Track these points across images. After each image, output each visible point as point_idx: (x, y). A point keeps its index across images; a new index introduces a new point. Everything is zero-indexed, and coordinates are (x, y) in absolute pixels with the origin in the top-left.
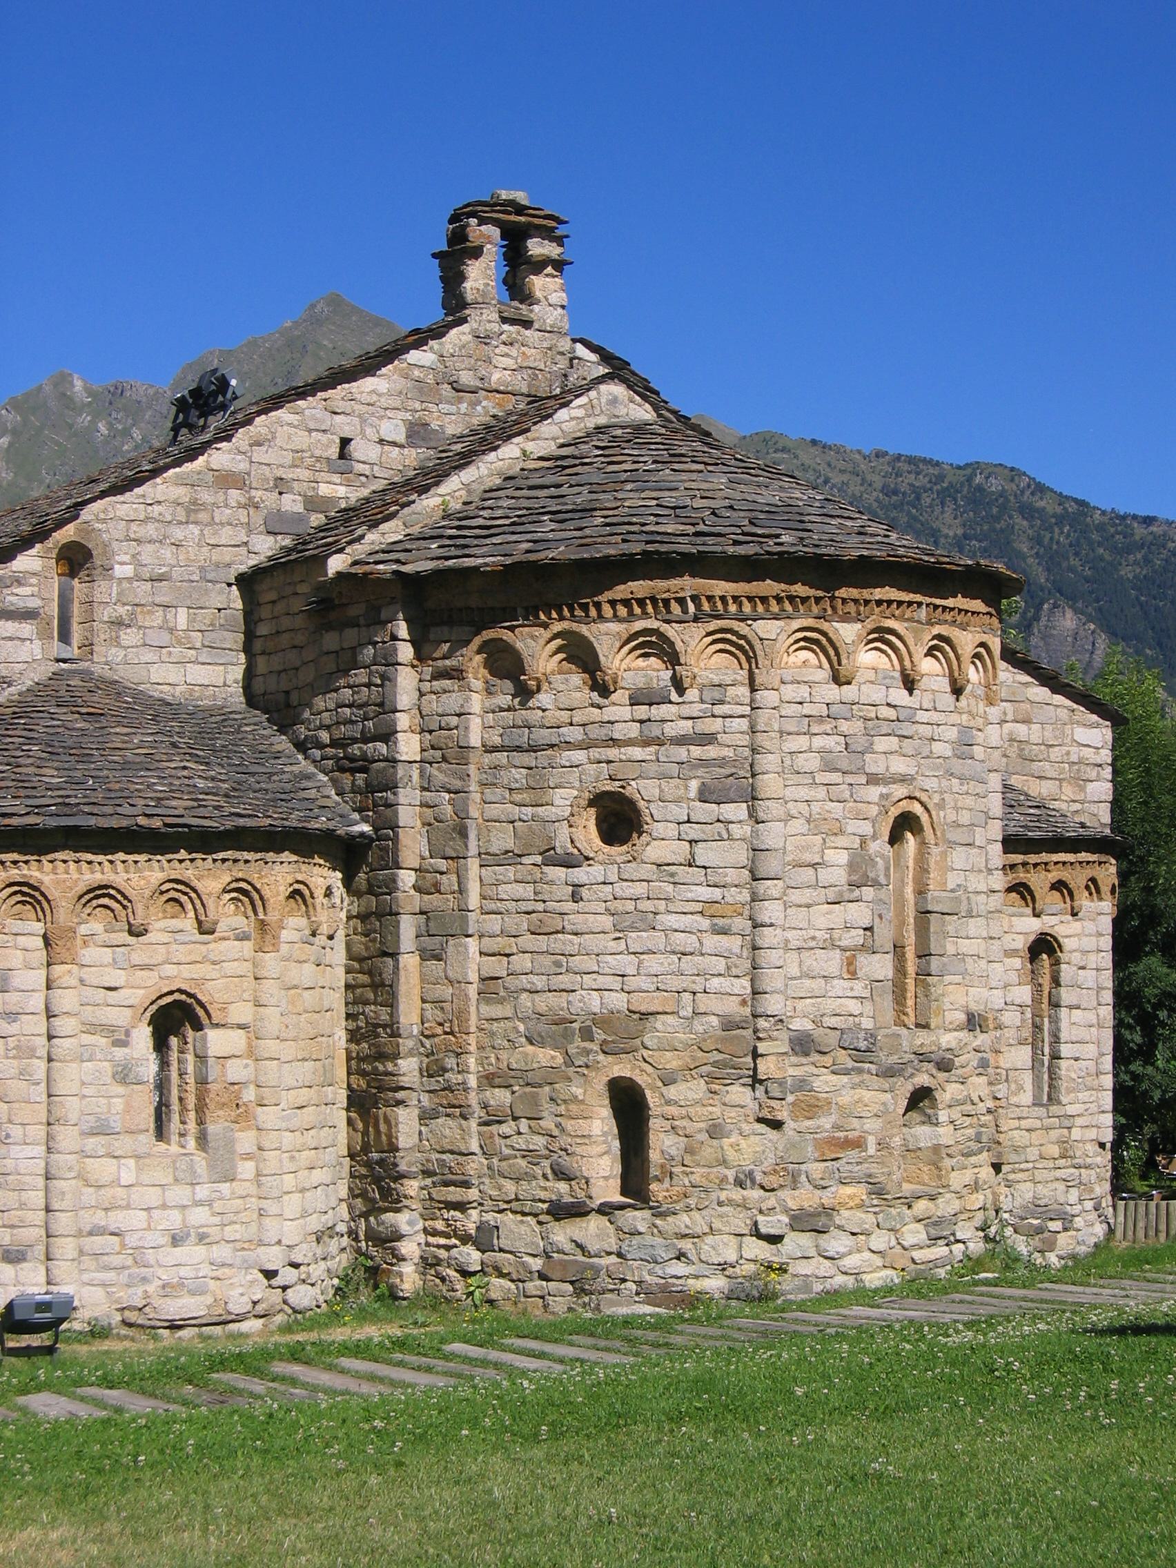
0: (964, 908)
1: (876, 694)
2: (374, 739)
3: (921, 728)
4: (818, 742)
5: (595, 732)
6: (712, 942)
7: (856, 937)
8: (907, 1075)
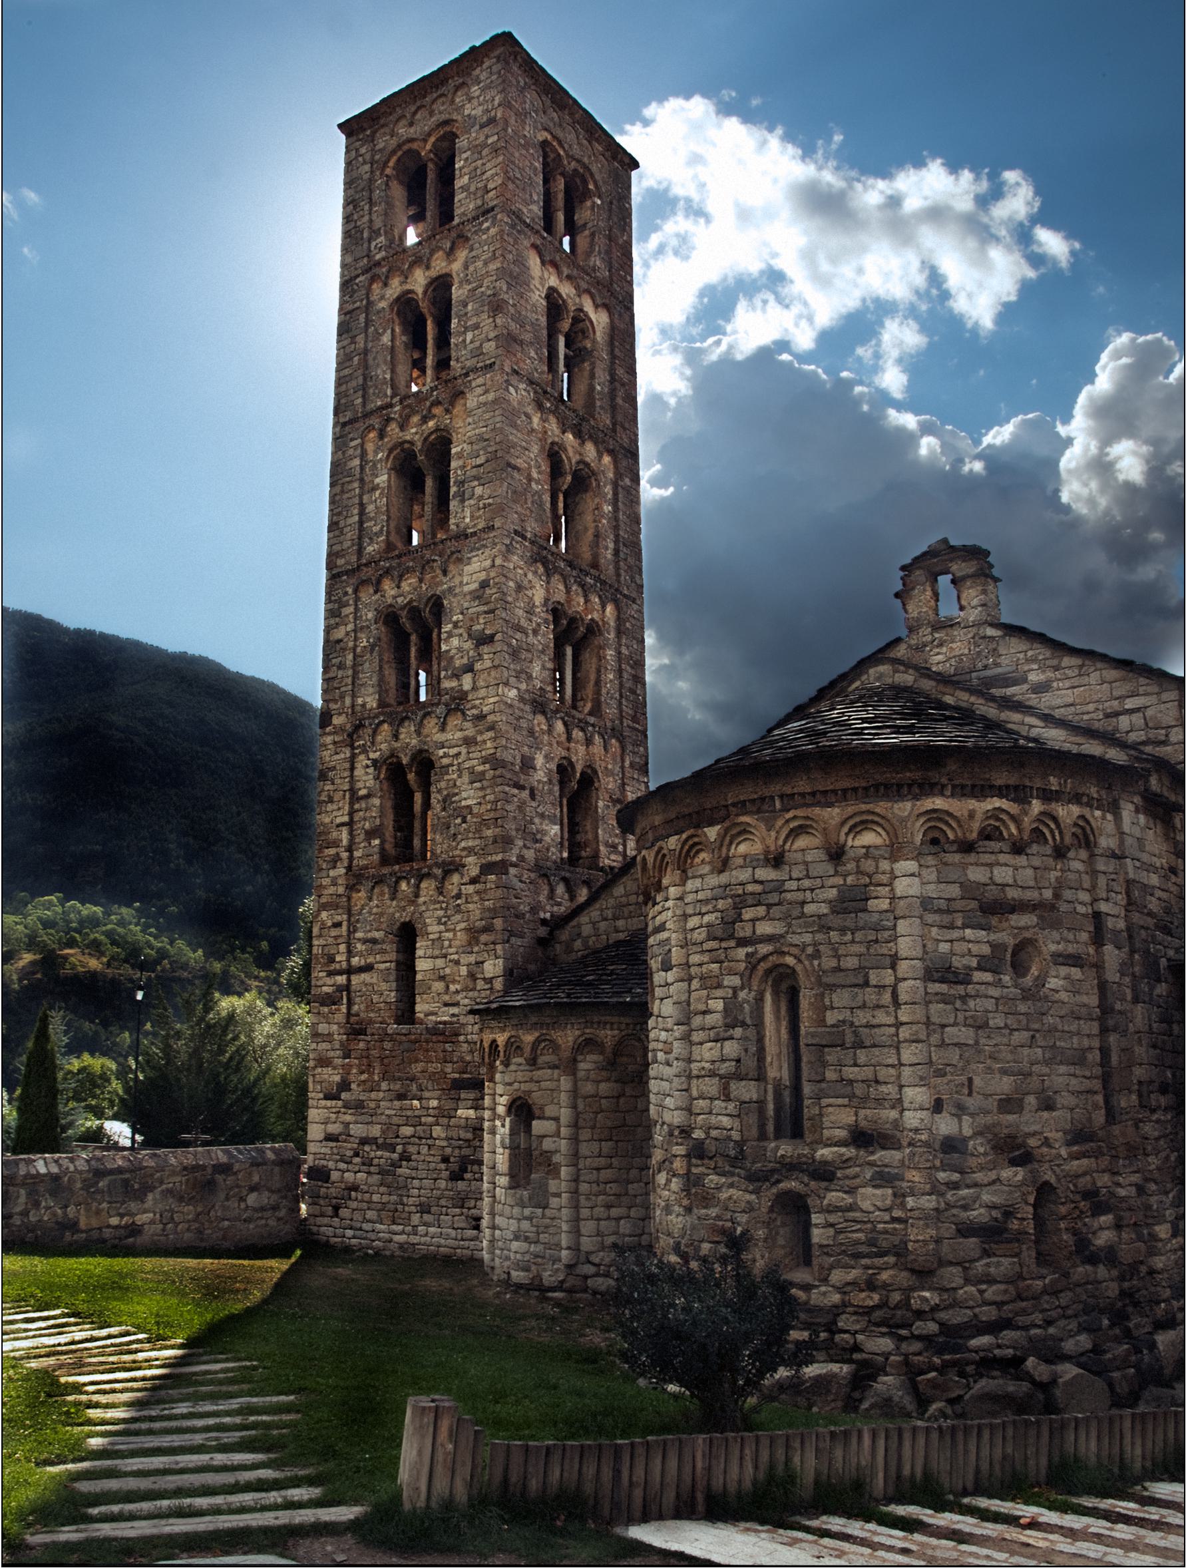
0: (849, 1039)
1: (745, 875)
3: (788, 896)
4: (706, 919)
8: (773, 1180)
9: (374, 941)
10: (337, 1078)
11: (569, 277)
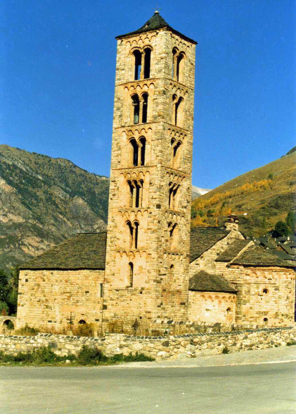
2: (238, 281)
5: (264, 283)
6: (276, 305)
7: (287, 305)
9: (166, 268)
10: (160, 302)
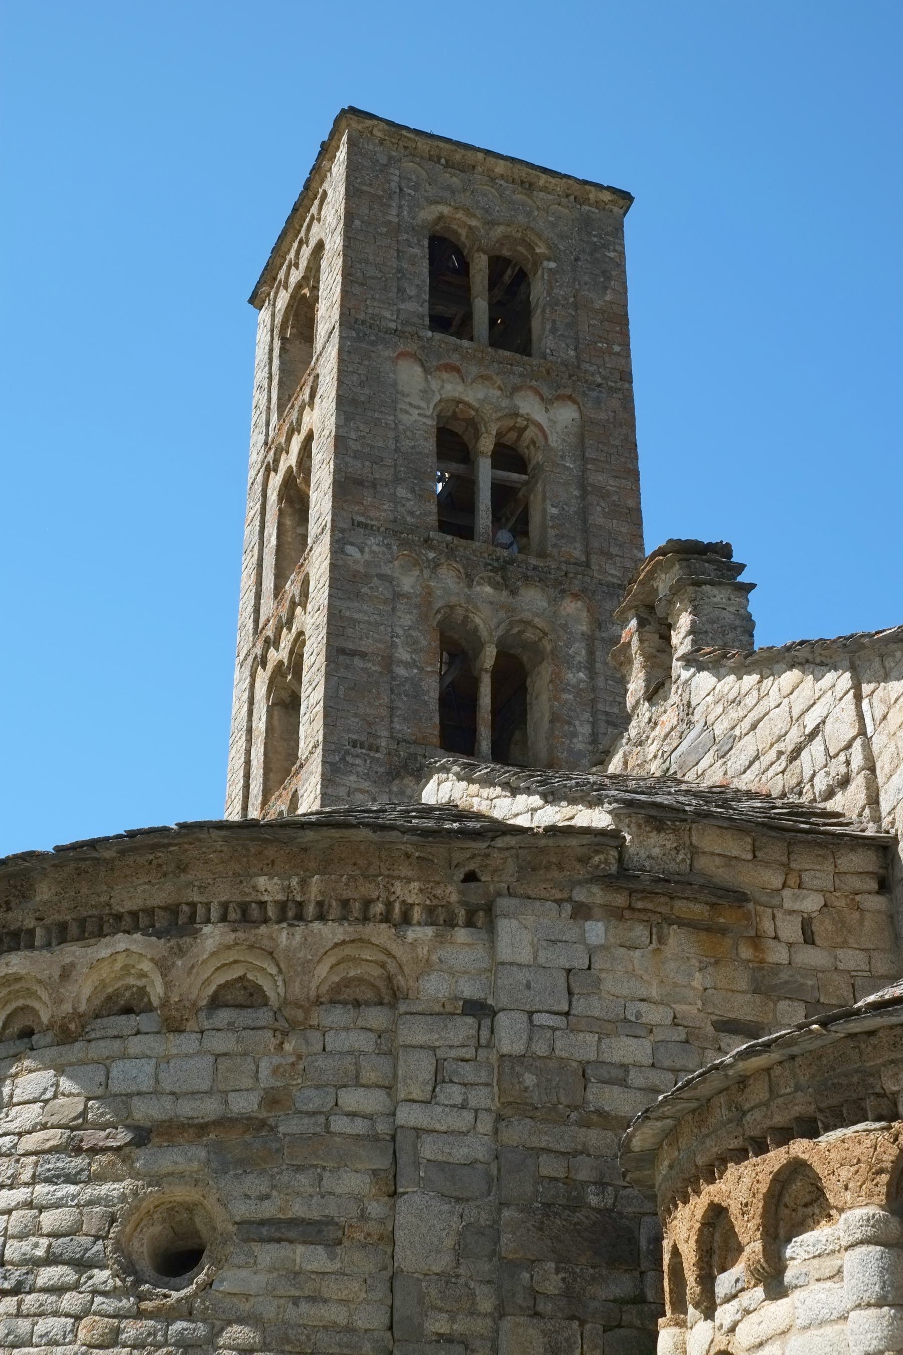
11: (484, 378)
